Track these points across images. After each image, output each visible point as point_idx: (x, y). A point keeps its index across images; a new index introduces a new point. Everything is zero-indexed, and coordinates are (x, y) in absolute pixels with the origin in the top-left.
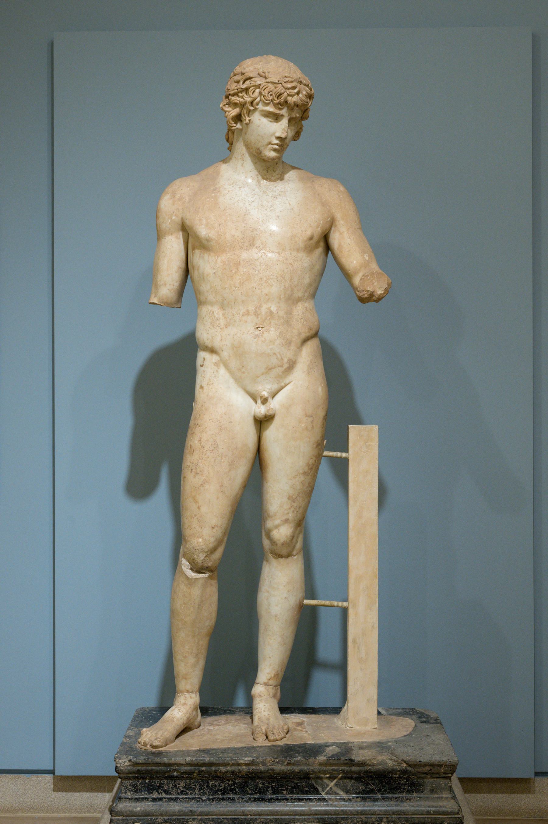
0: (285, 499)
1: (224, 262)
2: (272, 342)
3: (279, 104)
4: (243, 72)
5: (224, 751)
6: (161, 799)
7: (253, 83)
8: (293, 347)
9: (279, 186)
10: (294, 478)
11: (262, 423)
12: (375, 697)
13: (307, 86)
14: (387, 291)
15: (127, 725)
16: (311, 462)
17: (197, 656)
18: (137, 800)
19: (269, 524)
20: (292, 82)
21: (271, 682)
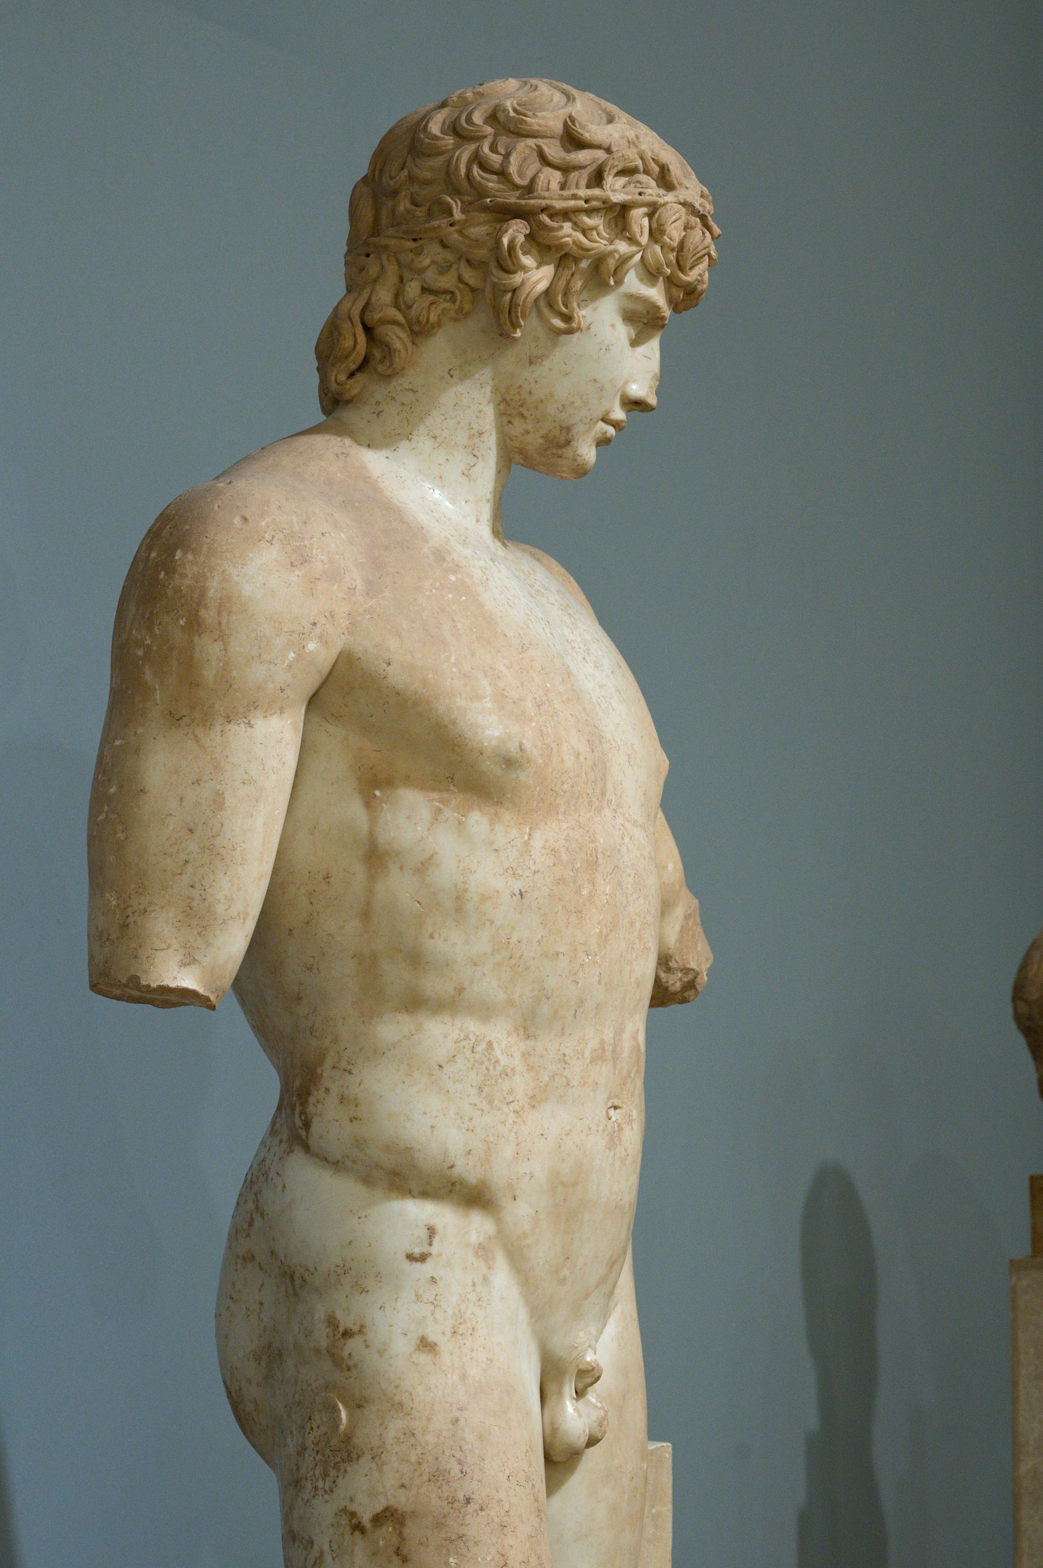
1: (554, 852)
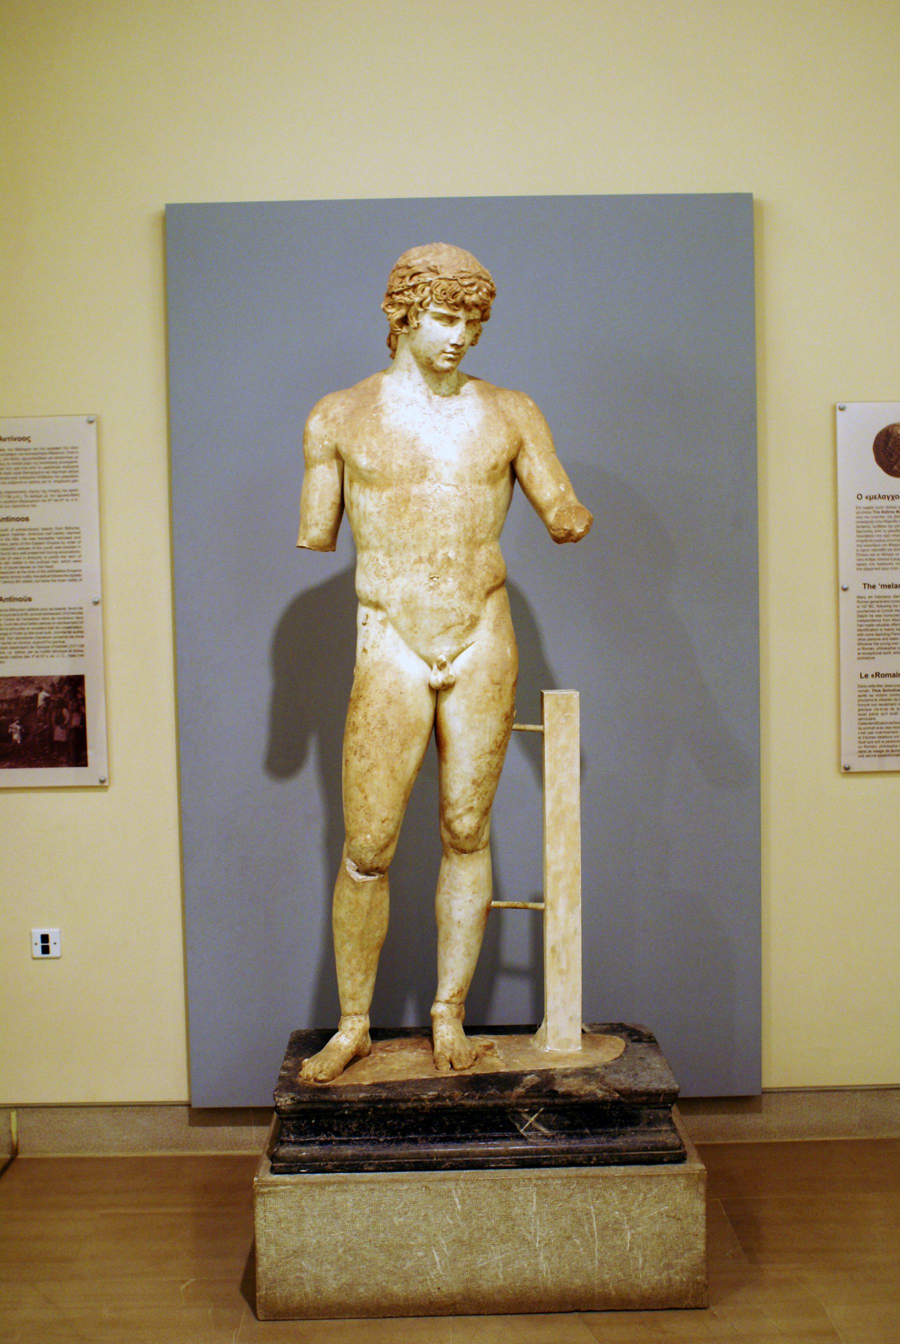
0: (469, 784)
1: (390, 499)
2: (450, 595)
3: (455, 304)
4: (410, 265)
5: (403, 1084)
6: (330, 1142)
7: (422, 280)
8: (475, 601)
9: (455, 403)
10: (479, 758)
11: (438, 692)
12: (579, 1014)
13: (488, 281)
14: (587, 528)
15: (283, 1055)
16: (500, 738)
17: (366, 972)
18: (302, 1144)
19: (450, 814)
20: (470, 278)
21: (454, 1000)
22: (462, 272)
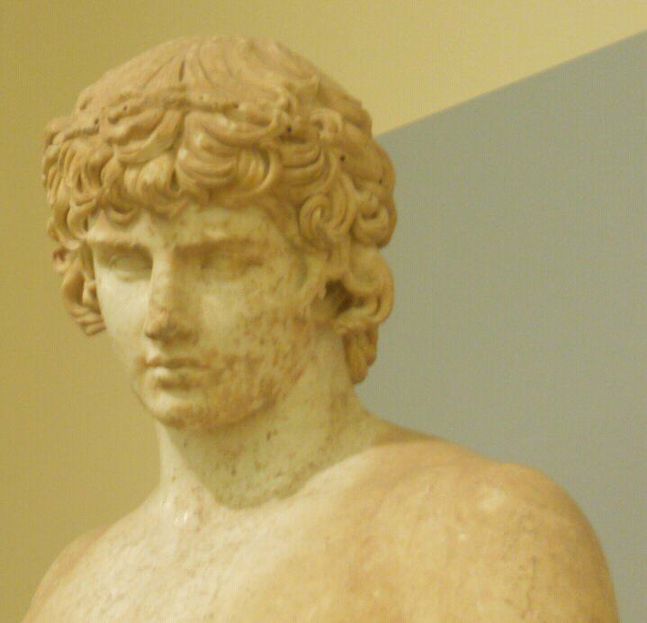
20: (136, 111)
22: (123, 98)
